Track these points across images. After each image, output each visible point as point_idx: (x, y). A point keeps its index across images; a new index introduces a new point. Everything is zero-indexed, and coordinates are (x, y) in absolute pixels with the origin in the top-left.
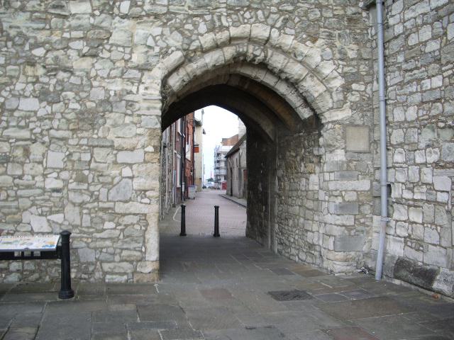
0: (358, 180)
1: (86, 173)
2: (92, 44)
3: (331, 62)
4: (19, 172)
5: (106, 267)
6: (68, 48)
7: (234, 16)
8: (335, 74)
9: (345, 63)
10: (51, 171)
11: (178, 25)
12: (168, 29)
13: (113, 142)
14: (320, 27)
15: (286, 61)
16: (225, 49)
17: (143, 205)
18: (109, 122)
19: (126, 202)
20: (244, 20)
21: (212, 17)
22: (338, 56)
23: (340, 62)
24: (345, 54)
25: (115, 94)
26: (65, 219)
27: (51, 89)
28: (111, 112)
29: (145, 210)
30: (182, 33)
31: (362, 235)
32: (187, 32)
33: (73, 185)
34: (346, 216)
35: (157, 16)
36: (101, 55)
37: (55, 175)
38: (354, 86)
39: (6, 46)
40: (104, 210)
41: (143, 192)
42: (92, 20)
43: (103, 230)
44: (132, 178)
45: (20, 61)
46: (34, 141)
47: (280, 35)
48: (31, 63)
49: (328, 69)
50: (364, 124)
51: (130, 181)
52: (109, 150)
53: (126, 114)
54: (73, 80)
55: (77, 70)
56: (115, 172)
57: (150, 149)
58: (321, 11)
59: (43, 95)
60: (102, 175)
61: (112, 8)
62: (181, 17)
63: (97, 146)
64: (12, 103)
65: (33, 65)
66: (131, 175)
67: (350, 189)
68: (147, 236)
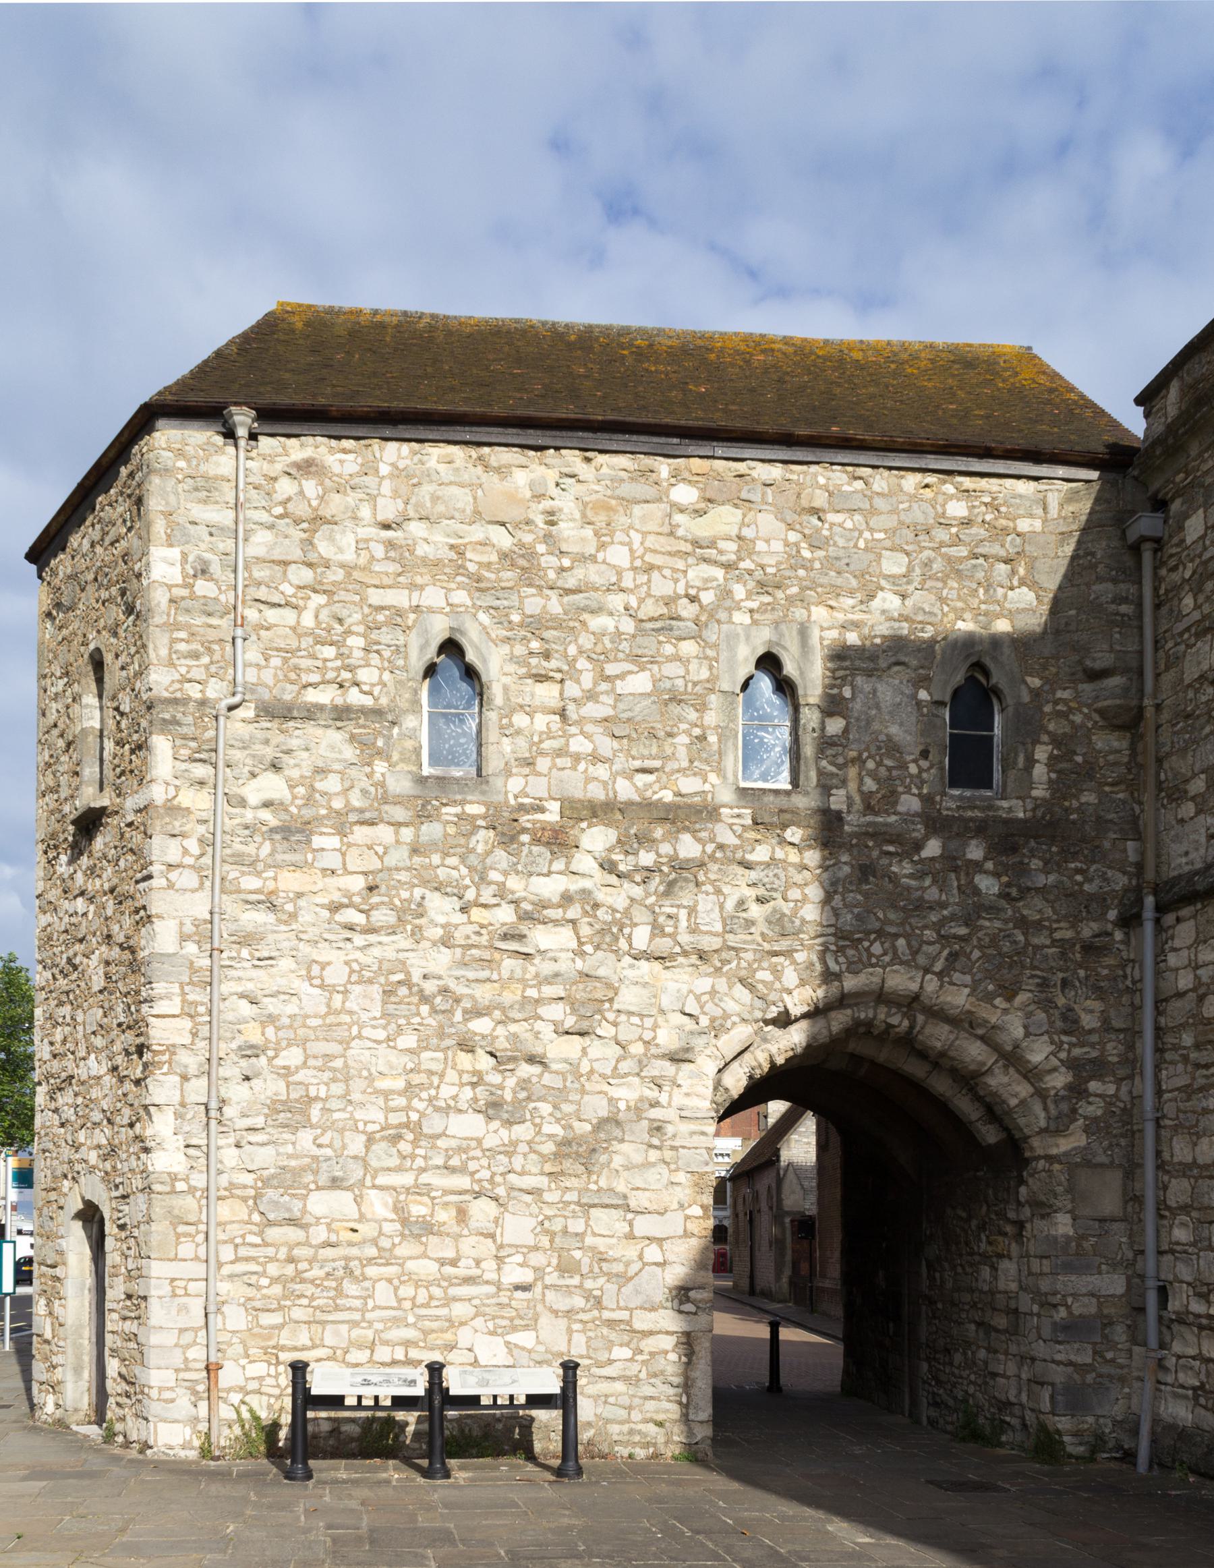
0: (1100, 1273)
1: (577, 1254)
2: (582, 1011)
3: (1046, 1038)
4: (450, 1254)
7: (850, 952)
8: (1055, 1062)
9: (1074, 1040)
11: (743, 973)
12: (724, 979)
13: (625, 1197)
14: (1023, 967)
15: (952, 1037)
16: (833, 1014)
18: (618, 1160)
20: (869, 958)
22: (1059, 1024)
23: (1065, 1038)
24: (1076, 1021)
25: (629, 1108)
26: (539, 1342)
27: (508, 1096)
28: (622, 1141)
30: (751, 988)
32: (760, 986)
33: (552, 1278)
34: (1076, 1346)
35: (702, 956)
37: (519, 1258)
38: (1093, 1086)
39: (418, 1014)
40: (611, 1323)
42: (579, 964)
43: (611, 1362)
47: (941, 987)
49: (1038, 1053)
50: (1112, 1162)
51: (658, 1270)
53: (651, 1146)
54: (547, 1079)
55: (554, 1060)
56: (631, 1252)
57: (696, 1211)
59: (493, 1108)
60: (604, 1260)
62: (749, 956)
63: (594, 1206)
64: (434, 1124)
67: (1084, 1291)
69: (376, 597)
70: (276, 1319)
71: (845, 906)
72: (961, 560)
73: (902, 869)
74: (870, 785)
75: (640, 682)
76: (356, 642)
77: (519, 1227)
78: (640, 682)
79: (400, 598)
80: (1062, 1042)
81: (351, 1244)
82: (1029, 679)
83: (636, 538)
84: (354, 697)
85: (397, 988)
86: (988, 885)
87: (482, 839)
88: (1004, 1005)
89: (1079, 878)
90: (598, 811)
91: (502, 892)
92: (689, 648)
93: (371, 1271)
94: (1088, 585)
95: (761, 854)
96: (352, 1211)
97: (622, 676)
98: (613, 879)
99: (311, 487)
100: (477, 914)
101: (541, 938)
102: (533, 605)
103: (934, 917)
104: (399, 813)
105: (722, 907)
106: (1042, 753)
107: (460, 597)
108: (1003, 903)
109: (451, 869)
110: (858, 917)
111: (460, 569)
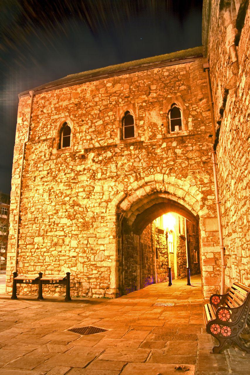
0: (214, 246)
1: (86, 249)
4: (60, 250)
5: (94, 291)
6: (78, 196)
7: (146, 172)
8: (198, 192)
9: (203, 186)
10: (72, 248)
11: (121, 180)
13: (96, 235)
14: (188, 170)
16: (145, 187)
17: (109, 263)
19: (102, 261)
20: (151, 172)
21: (136, 174)
22: (199, 183)
23: (200, 186)
24: (203, 181)
25: (97, 214)
26: (77, 269)
29: (109, 264)
31: (218, 276)
34: (208, 266)
35: (112, 178)
36: (90, 197)
37: (73, 250)
38: (209, 197)
39: (55, 198)
41: (108, 257)
43: (92, 274)
44: (104, 250)
45: (60, 203)
46: (66, 236)
51: (103, 252)
52: (95, 238)
53: (101, 223)
57: (111, 237)
58: (188, 162)
59: (69, 217)
61: (94, 176)
62: (123, 176)
65: (65, 204)
66: (103, 249)
67: (209, 251)
68: (111, 277)
70: (28, 265)
71: (144, 161)
72: (168, 83)
74: (151, 134)
75: (101, 122)
77: (74, 243)
78: (101, 122)
79: (56, 117)
80: (200, 187)
81: (42, 248)
82: (185, 104)
83: (100, 95)
87: (69, 159)
88: (185, 179)
89: (201, 146)
91: (72, 170)
93: (45, 254)
94: (196, 82)
96: (42, 241)
97: (96, 122)
98: (94, 164)
100: (68, 176)
103: (165, 161)
105: (116, 166)
106: (190, 120)
107: (67, 114)
108: (182, 155)
110: (147, 164)
111: (67, 108)
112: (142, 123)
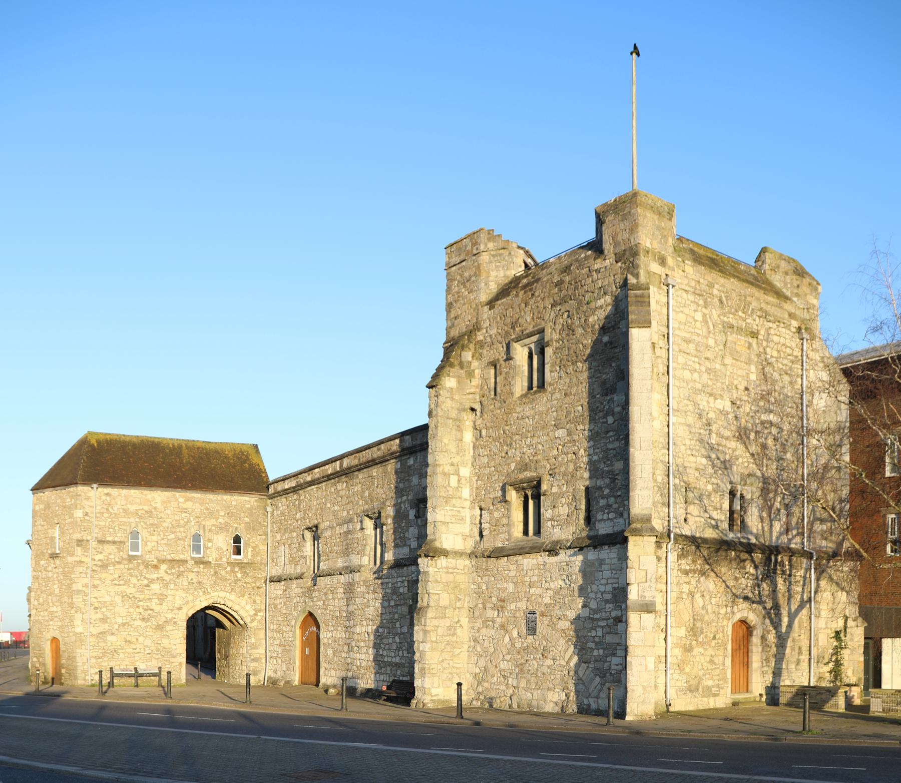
48: (138, 607)
69: (120, 520)
73: (223, 573)
75: (172, 536)
76: (117, 528)
79: (125, 520)
84: (116, 539)
85: (125, 596)
86: (239, 575)
87: (142, 567)
90: (163, 561)
91: (145, 578)
92: (182, 529)
95: (196, 570)
99: (108, 498)
101: (153, 586)
102: (151, 521)
104: (125, 562)
106: (250, 550)
107: (137, 520)
109: (136, 572)
112: (210, 545)
